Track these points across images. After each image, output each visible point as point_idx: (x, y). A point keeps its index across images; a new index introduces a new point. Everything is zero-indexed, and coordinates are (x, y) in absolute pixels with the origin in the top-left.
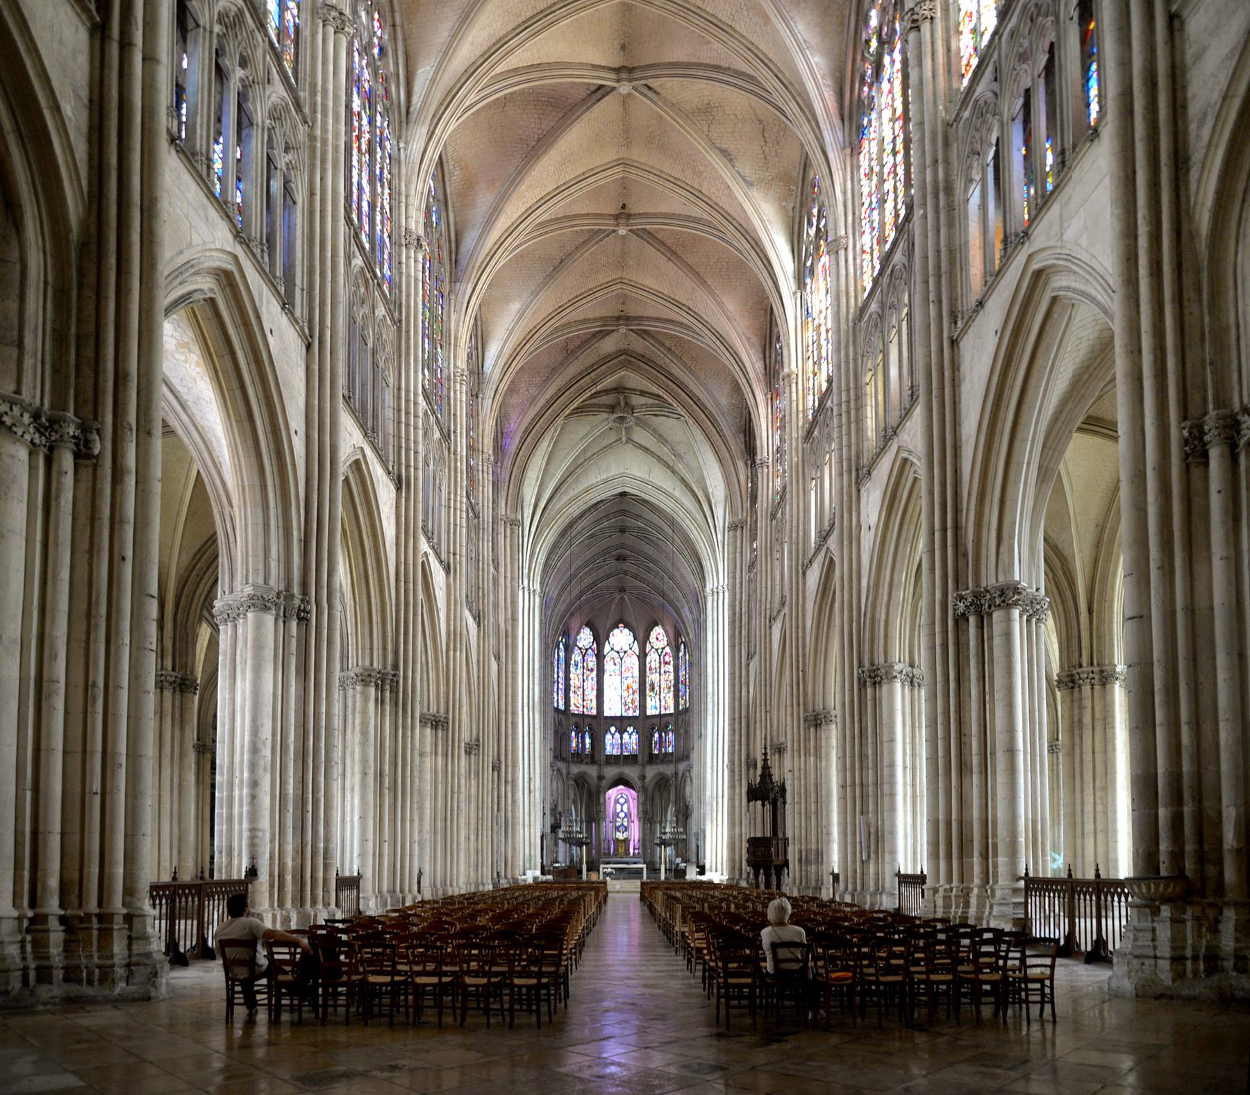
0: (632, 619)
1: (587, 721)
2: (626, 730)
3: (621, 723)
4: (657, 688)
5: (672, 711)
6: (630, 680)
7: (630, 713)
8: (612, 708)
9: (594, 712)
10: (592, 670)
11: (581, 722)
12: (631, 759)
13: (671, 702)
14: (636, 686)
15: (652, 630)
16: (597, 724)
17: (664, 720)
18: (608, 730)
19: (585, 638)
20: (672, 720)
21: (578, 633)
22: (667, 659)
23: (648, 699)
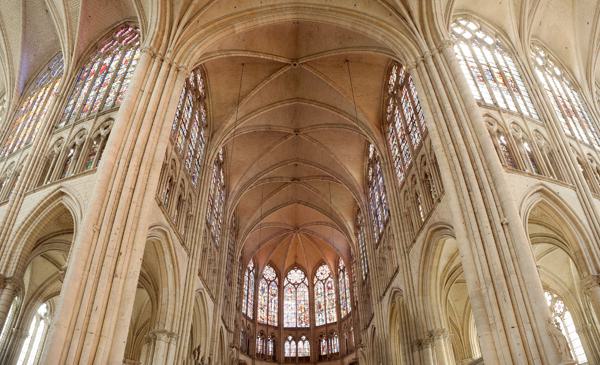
0: (302, 262)
1: (271, 330)
2: (300, 339)
3: (297, 333)
4: (323, 307)
5: (335, 320)
6: (303, 303)
7: (303, 325)
8: (290, 321)
9: (276, 324)
10: (275, 295)
11: (265, 329)
12: (306, 359)
13: (334, 315)
14: (307, 307)
15: (318, 268)
16: (278, 333)
17: (330, 328)
18: (286, 339)
19: (269, 273)
20: (335, 328)
21: (263, 268)
22: (330, 285)
23: (317, 315)
